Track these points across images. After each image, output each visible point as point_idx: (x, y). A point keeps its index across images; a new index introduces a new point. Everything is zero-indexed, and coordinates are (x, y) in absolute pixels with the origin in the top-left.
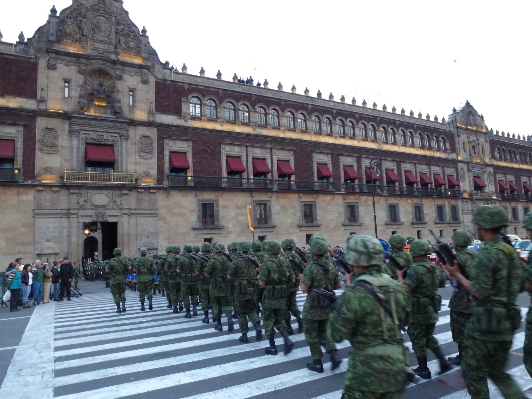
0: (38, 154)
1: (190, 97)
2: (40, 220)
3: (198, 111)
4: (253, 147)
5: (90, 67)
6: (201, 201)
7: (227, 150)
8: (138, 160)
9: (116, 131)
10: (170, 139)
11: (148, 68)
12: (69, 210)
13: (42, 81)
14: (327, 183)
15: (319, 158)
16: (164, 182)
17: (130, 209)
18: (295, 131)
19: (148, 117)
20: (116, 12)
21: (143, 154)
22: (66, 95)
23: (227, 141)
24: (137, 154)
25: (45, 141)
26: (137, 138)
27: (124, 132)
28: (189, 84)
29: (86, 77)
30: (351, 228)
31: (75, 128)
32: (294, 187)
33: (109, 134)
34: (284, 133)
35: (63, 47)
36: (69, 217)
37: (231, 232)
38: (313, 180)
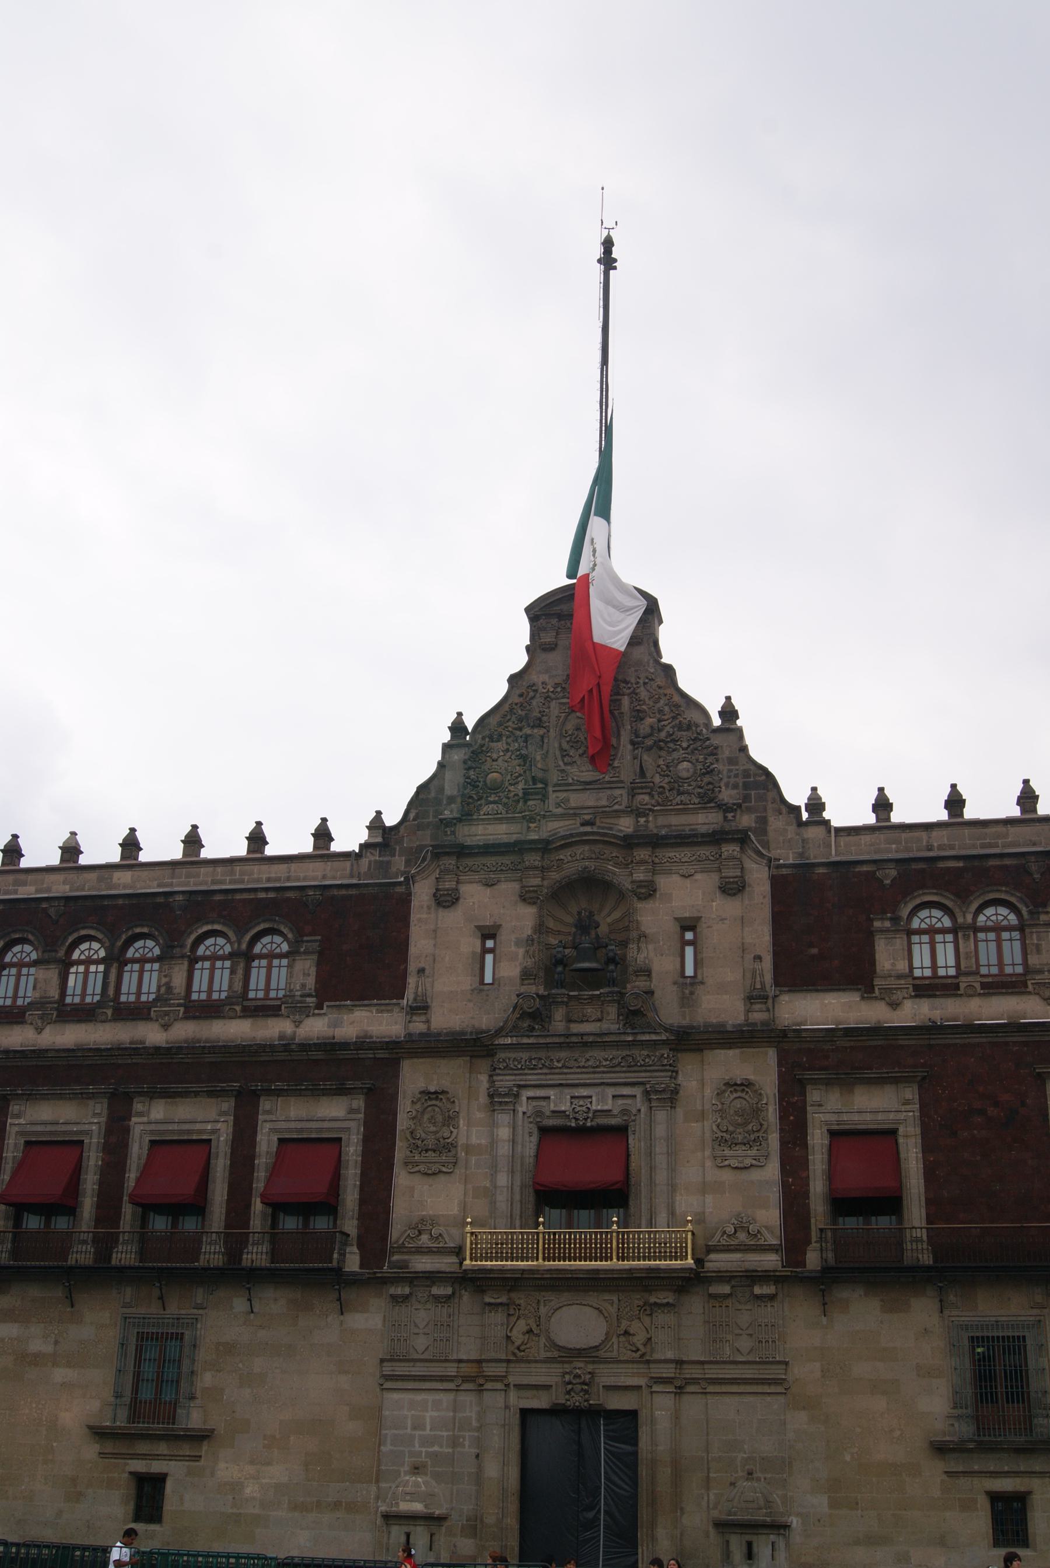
0: (401, 1178)
1: (905, 912)
2: (396, 1396)
3: (946, 956)
5: (555, 876)
6: (966, 1327)
9: (632, 1077)
10: (828, 1083)
11: (742, 839)
12: (479, 1362)
13: (419, 945)
17: (680, 1363)
19: (748, 1011)
20: (633, 680)
21: (727, 1152)
24: (708, 1153)
25: (420, 1133)
26: (708, 1092)
27: (662, 1079)
28: (898, 861)
29: (541, 909)
31: (506, 1082)
33: (611, 1091)
35: (480, 829)
36: (480, 1390)
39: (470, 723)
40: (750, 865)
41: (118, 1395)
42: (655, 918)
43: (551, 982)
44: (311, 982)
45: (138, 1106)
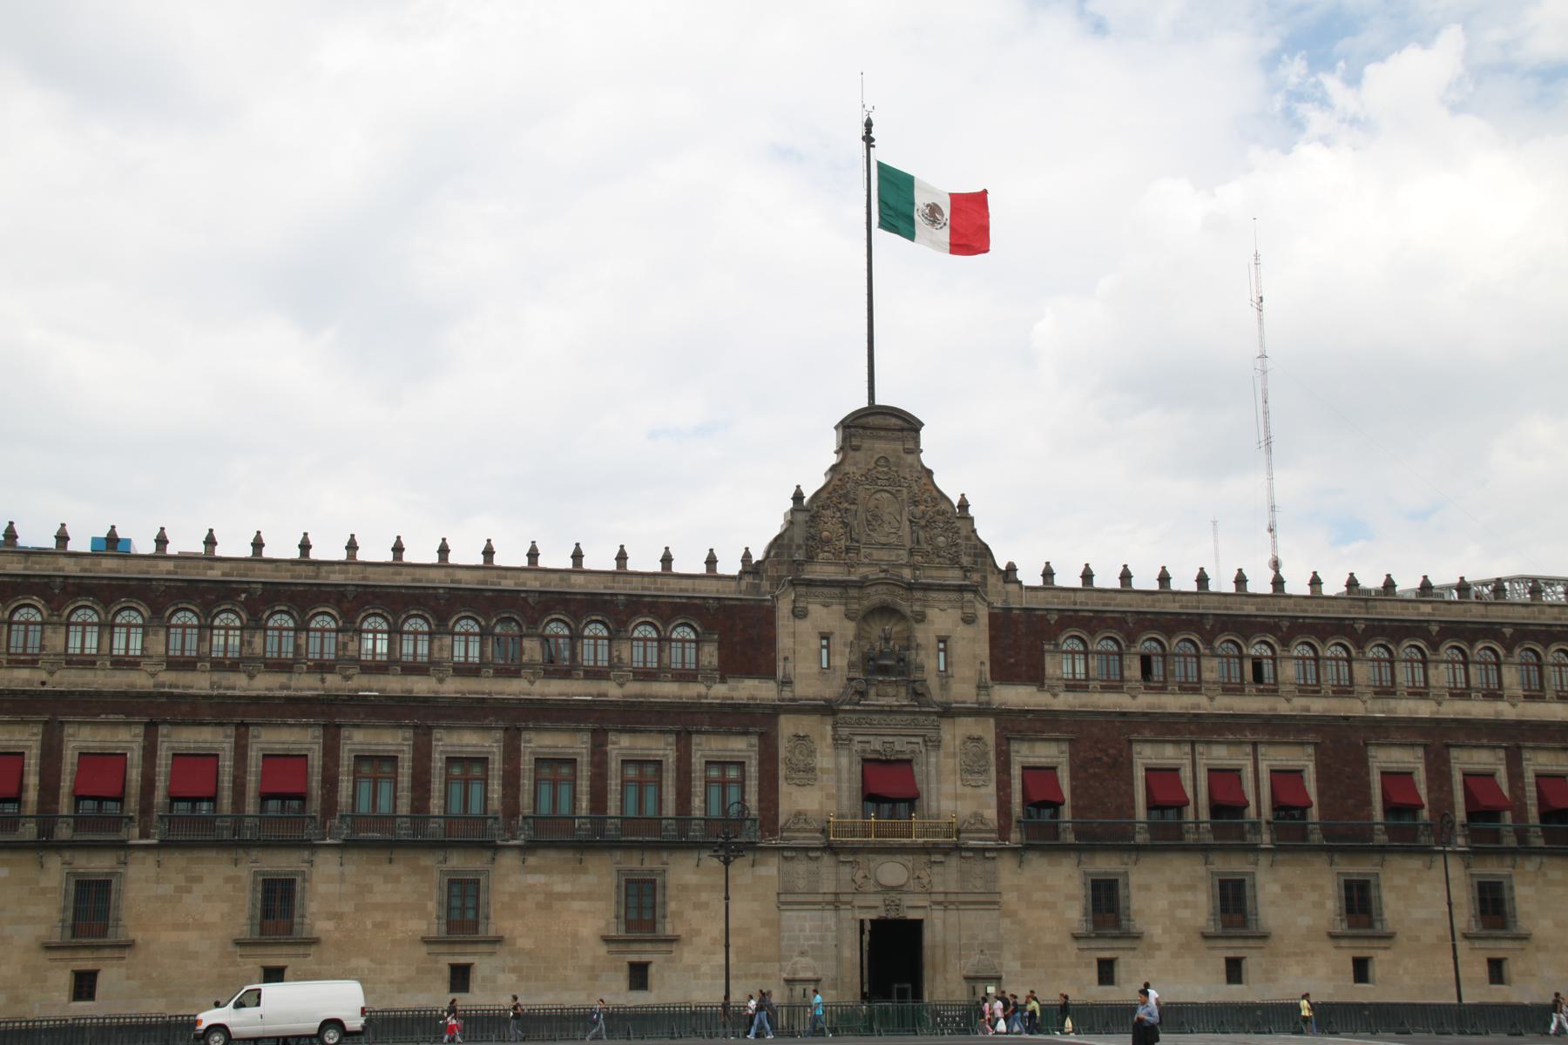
0: (783, 787)
1: (1061, 640)
4: (1209, 743)
7: (1146, 756)
8: (960, 789)
10: (1022, 740)
11: (973, 589)
12: (836, 894)
13: (784, 642)
14: (1408, 829)
15: (1385, 758)
16: (1013, 836)
18: (1318, 692)
22: (825, 665)
23: (1148, 734)
26: (957, 742)
27: (931, 734)
30: (1490, 944)
31: (844, 732)
32: (1316, 838)
34: (1288, 700)
35: (818, 568)
36: (837, 908)
37: (1159, 947)
38: (1370, 816)
39: (808, 494)
40: (978, 605)
41: (617, 917)
42: (925, 635)
43: (867, 671)
44: (715, 661)
45: (612, 737)
